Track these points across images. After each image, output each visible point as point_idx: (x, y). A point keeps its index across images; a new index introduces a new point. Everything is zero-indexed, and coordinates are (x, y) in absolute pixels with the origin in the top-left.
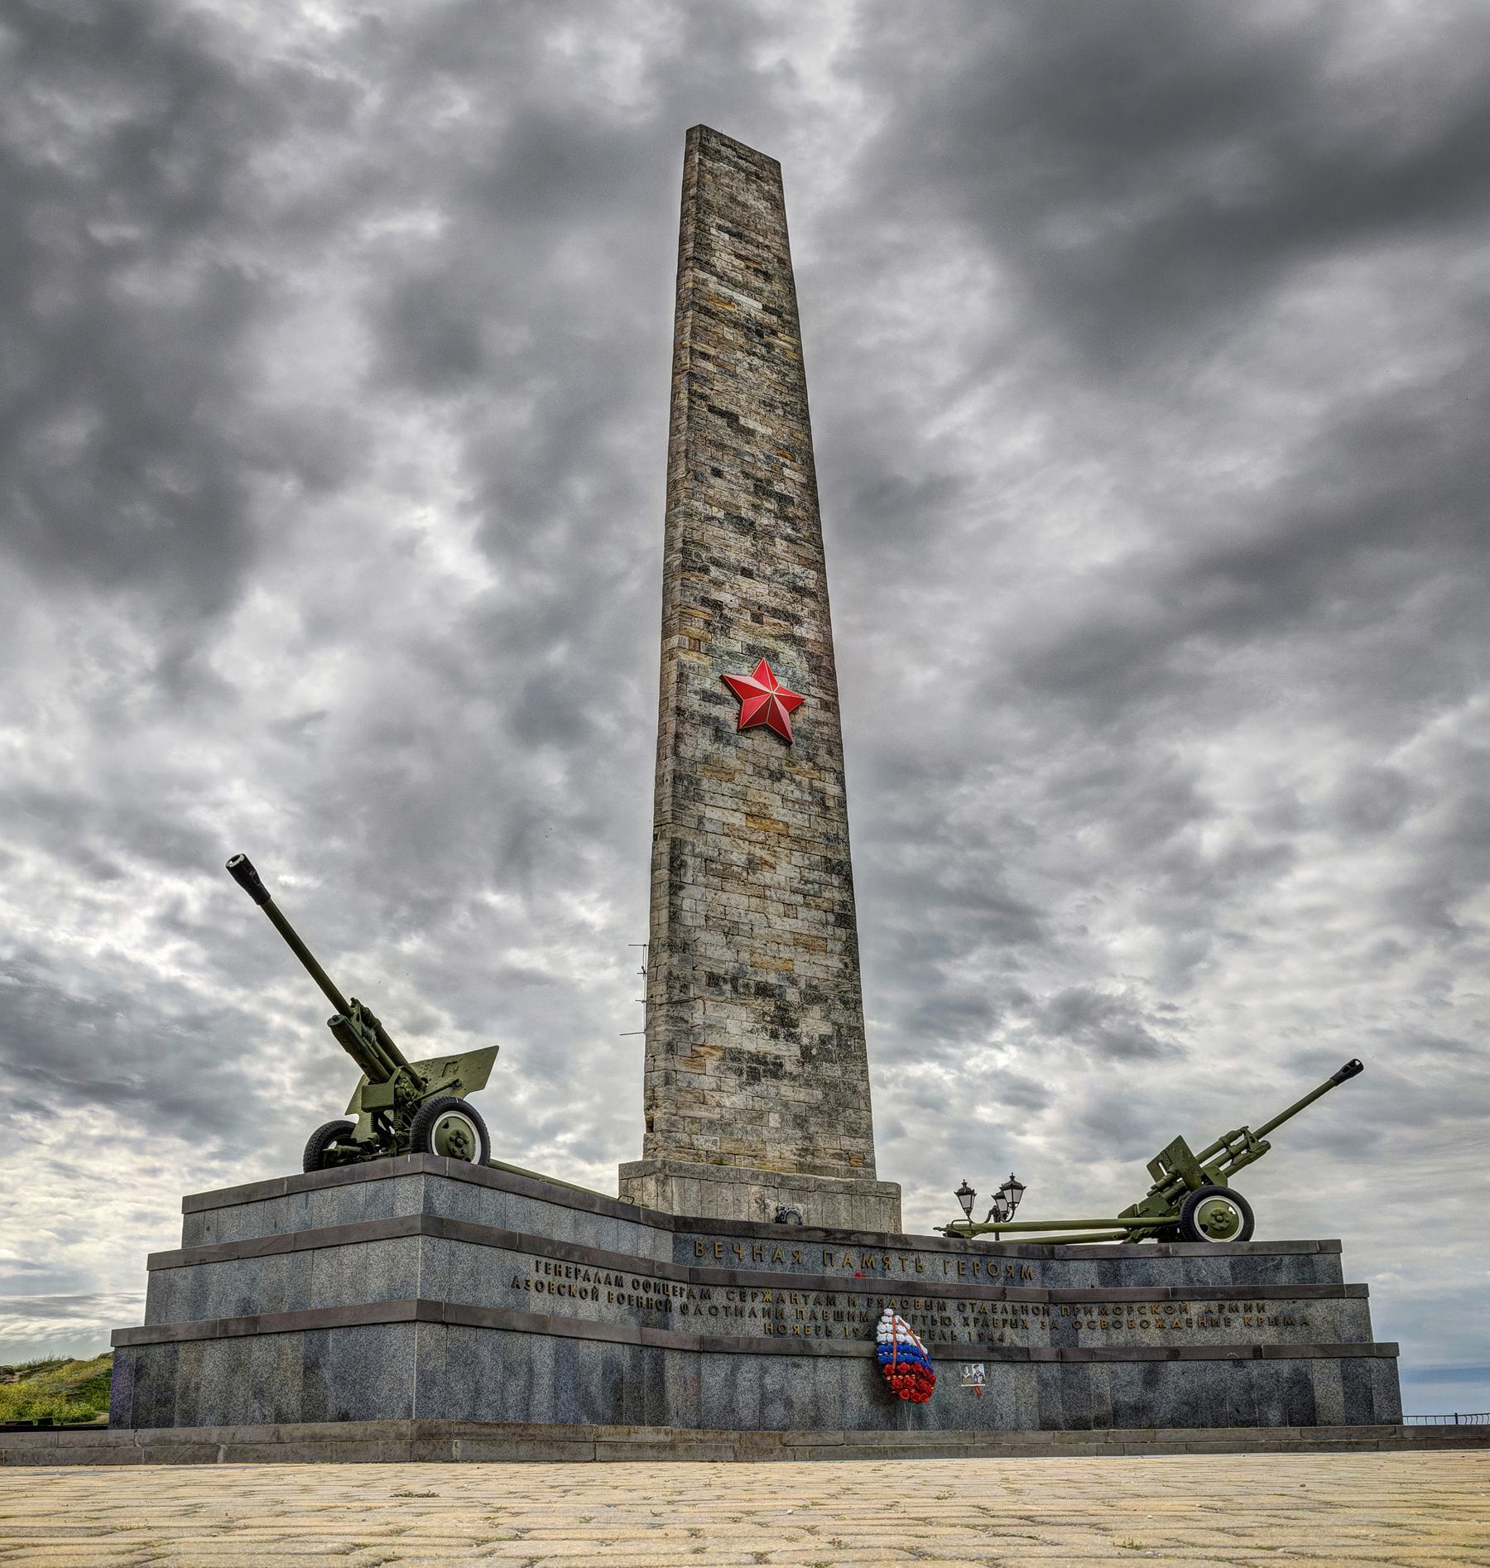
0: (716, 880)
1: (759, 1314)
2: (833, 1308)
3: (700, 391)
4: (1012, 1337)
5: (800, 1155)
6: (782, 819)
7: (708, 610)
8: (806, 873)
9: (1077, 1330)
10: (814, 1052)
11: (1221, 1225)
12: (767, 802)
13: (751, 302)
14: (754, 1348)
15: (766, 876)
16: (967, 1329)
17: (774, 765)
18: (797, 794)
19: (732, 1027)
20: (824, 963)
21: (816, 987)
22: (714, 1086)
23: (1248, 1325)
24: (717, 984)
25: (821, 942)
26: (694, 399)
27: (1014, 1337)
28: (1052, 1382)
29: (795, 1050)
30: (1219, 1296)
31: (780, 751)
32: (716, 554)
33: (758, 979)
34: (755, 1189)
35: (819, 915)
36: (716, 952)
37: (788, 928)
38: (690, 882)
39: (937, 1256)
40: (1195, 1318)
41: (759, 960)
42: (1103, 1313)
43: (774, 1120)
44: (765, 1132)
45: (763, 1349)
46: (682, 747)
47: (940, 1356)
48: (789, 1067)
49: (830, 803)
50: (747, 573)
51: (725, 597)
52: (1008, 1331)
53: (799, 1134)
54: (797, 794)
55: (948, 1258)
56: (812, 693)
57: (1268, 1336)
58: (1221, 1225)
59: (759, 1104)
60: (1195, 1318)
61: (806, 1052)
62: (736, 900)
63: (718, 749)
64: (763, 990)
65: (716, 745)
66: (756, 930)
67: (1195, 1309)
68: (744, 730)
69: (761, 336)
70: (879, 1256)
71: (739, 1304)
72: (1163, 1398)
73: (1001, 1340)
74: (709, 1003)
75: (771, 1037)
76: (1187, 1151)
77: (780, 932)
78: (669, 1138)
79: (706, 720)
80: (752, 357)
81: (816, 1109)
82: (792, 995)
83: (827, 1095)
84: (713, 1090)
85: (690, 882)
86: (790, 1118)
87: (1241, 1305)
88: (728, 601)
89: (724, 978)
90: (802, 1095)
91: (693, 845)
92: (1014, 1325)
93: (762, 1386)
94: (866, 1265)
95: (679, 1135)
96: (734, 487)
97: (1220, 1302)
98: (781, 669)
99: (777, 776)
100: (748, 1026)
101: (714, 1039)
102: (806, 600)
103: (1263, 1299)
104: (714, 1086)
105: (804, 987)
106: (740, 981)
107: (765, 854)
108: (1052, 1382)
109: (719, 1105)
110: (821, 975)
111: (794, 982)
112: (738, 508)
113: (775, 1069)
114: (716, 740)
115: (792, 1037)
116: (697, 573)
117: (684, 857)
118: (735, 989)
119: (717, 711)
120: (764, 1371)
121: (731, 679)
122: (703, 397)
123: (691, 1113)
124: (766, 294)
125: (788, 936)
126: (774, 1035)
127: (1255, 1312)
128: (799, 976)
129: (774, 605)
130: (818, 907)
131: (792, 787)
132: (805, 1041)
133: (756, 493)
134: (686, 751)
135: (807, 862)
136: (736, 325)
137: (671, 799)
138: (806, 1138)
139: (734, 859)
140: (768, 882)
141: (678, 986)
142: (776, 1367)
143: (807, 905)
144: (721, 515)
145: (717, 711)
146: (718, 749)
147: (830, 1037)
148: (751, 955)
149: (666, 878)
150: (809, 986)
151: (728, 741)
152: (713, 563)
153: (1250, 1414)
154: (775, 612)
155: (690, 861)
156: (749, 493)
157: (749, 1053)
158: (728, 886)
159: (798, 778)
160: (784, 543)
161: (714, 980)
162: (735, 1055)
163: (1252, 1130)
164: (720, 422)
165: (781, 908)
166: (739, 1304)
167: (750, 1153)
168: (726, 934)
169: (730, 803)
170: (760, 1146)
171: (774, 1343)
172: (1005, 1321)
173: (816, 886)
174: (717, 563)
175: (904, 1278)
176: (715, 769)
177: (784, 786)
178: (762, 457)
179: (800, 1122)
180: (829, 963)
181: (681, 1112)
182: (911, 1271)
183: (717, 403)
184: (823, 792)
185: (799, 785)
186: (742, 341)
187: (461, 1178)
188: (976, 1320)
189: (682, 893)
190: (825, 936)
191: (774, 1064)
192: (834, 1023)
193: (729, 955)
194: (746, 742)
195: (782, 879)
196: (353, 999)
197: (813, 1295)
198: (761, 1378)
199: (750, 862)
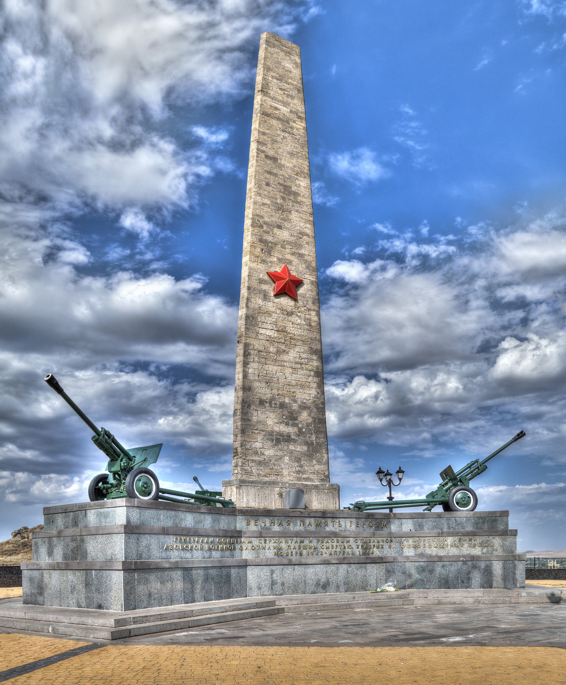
0: (263, 360)
1: (272, 548)
2: (302, 544)
3: (261, 149)
4: (377, 553)
5: (297, 473)
6: (293, 332)
7: (262, 244)
8: (302, 354)
10: (304, 430)
11: (464, 502)
12: (285, 325)
13: (285, 108)
14: (269, 563)
15: (285, 357)
16: (358, 550)
17: (289, 309)
18: (299, 321)
19: (270, 422)
20: (308, 392)
21: (305, 403)
22: (261, 446)
23: (470, 547)
24: (263, 404)
25: (308, 384)
26: (259, 152)
27: (377, 552)
28: (392, 570)
29: (296, 429)
31: (292, 303)
32: (266, 219)
33: (280, 401)
34: (277, 489)
35: (308, 373)
37: (293, 379)
38: (252, 361)
39: (347, 519)
40: (449, 544)
41: (281, 393)
43: (286, 459)
44: (282, 464)
45: (272, 563)
46: (250, 303)
47: (346, 562)
48: (293, 437)
49: (313, 324)
50: (279, 227)
51: (270, 238)
52: (375, 549)
53: (296, 464)
54: (299, 321)
55: (352, 520)
56: (306, 277)
58: (464, 502)
59: (280, 453)
61: (300, 430)
62: (272, 368)
63: (265, 303)
64: (282, 406)
65: (264, 302)
66: (280, 380)
67: (450, 540)
68: (277, 295)
69: (289, 123)
70: (323, 521)
71: (264, 545)
72: (434, 576)
73: (372, 553)
74: (259, 412)
75: (286, 424)
76: (452, 471)
77: (290, 381)
78: (243, 469)
79: (261, 291)
80: (284, 133)
81: (303, 454)
82: (295, 407)
84: (260, 448)
85: (252, 361)
86: (293, 458)
88: (271, 239)
89: (266, 402)
90: (299, 449)
91: (254, 345)
92: (378, 548)
93: (272, 578)
94: (318, 525)
95: (246, 468)
96: (275, 190)
98: (293, 268)
99: (290, 314)
100: (275, 420)
102: (305, 237)
104: (261, 446)
105: (300, 403)
106: (273, 402)
107: (283, 347)
108: (392, 570)
109: (263, 454)
110: (307, 398)
111: (295, 401)
112: (276, 199)
113: (288, 439)
114: (264, 300)
115: (294, 425)
116: (258, 228)
117: (250, 351)
118: (271, 406)
119: (264, 287)
120: (272, 572)
122: (263, 152)
123: (251, 458)
124: (291, 105)
125: (294, 382)
126: (287, 424)
127: (473, 541)
128: (298, 398)
129: (291, 240)
130: (307, 369)
131: (297, 318)
132: (300, 426)
133: (284, 193)
134: (251, 305)
135: (302, 350)
136: (278, 119)
137: (244, 326)
138: (300, 466)
139: (271, 350)
140: (286, 359)
141: (246, 405)
142: (278, 569)
143: (302, 368)
144: (269, 202)
145: (264, 287)
146: (265, 303)
147: (311, 423)
148: (278, 391)
151: (269, 300)
152: (265, 223)
153: (467, 584)
154: (289, 243)
155: (252, 352)
156: (280, 192)
157: (276, 432)
158: (268, 362)
159: (299, 314)
160: (296, 213)
161: (262, 402)
163: (480, 461)
165: (291, 370)
166: (264, 545)
167: (276, 473)
169: (270, 327)
170: (280, 470)
171: (277, 560)
172: (374, 546)
173: (306, 360)
174: (265, 223)
175: (333, 529)
176: (264, 312)
177: (294, 318)
178: (287, 176)
179: (298, 460)
180: (311, 392)
181: (247, 458)
182: (336, 526)
183: (269, 154)
184: (310, 319)
185: (300, 317)
186: (281, 126)
187: (142, 506)
188: (362, 546)
189: (248, 366)
190: (310, 381)
191: (287, 436)
192: (313, 418)
193: (268, 391)
195: (291, 358)
196: (102, 428)
197: (295, 539)
198: (272, 574)
199: (278, 351)
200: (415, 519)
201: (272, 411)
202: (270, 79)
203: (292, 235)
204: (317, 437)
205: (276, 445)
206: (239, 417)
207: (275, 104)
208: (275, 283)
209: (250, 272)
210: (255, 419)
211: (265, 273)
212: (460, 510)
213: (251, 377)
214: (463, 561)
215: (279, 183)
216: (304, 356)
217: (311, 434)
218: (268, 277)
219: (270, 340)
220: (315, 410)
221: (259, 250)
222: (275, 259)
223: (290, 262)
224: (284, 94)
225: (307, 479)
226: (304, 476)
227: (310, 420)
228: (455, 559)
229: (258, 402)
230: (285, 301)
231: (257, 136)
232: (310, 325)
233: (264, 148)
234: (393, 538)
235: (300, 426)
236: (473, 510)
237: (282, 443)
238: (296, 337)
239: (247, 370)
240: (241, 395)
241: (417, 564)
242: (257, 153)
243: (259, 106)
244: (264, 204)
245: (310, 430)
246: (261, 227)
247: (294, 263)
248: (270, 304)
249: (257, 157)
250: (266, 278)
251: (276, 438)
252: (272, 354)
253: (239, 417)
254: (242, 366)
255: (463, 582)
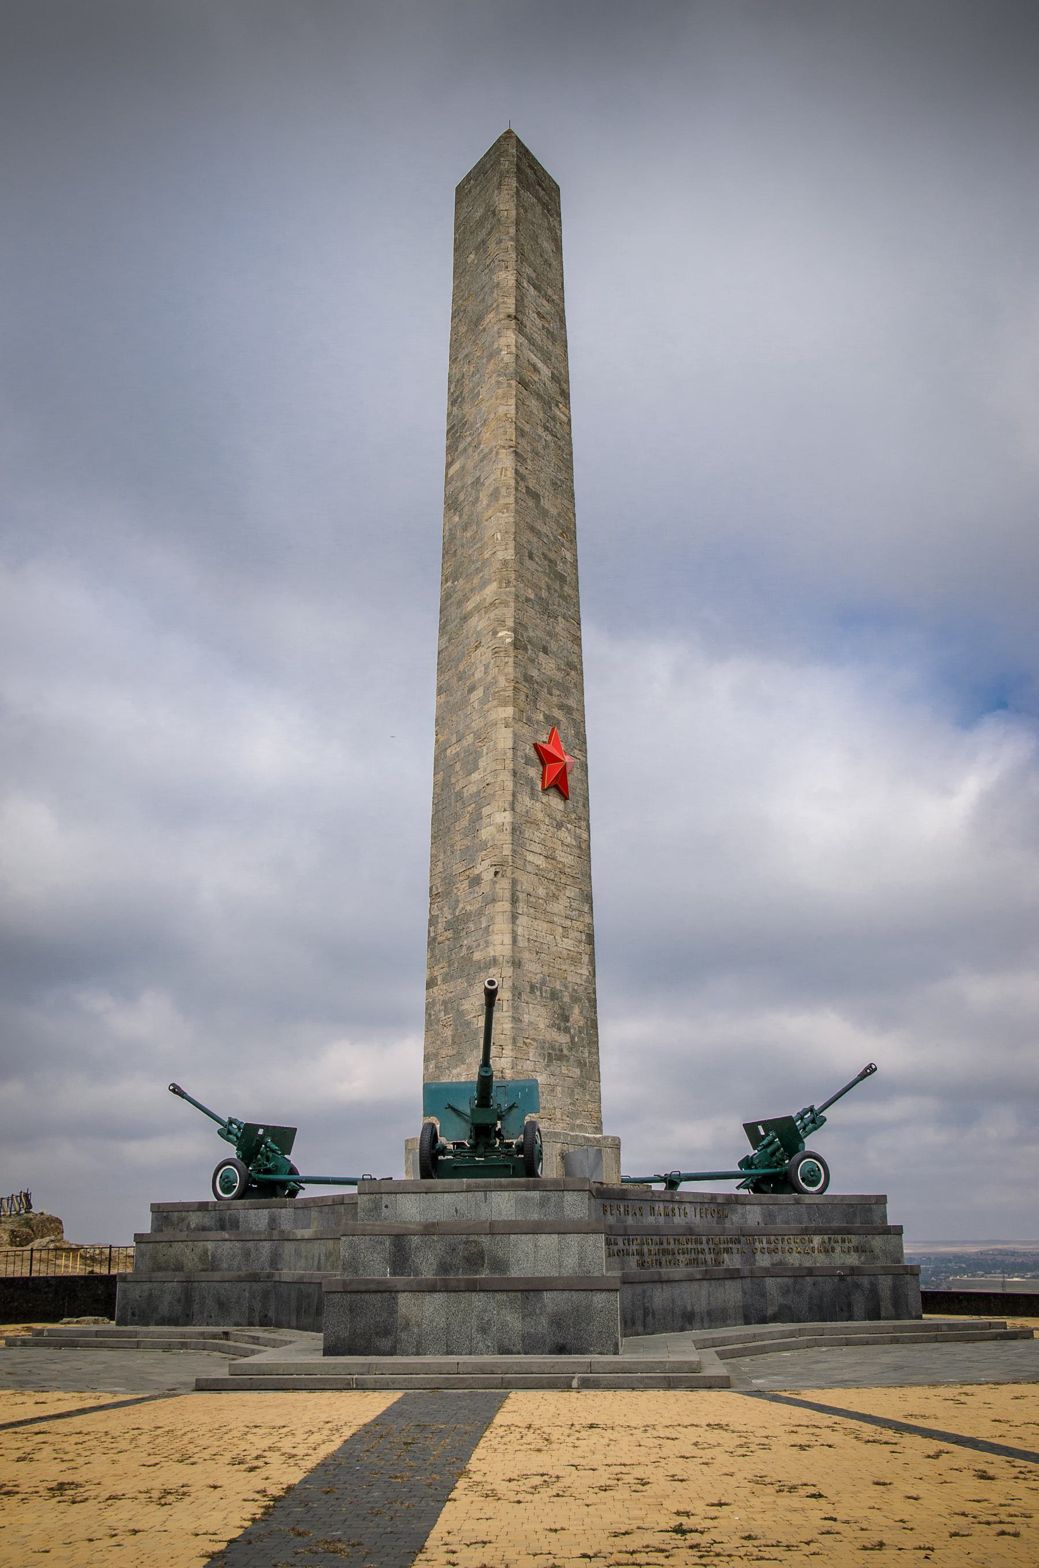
9: (755, 1253)
10: (576, 1040)
30: (829, 1232)
36: (533, 969)
40: (816, 1246)
41: (551, 971)
42: (769, 1242)
48: (565, 1052)
50: (545, 650)
51: (534, 673)
53: (569, 1101)
57: (853, 1260)
59: (552, 1081)
60: (816, 1246)
61: (572, 1038)
64: (554, 995)
67: (817, 1240)
83: (582, 1071)
84: (532, 1071)
87: (839, 1237)
97: (829, 1236)
99: (559, 826)
101: (532, 1033)
103: (851, 1234)
111: (566, 987)
115: (567, 1030)
121: (542, 748)
134: (519, 808)
144: (532, 597)
149: (509, 909)
150: (574, 990)
151: (537, 797)
154: (558, 685)
162: (542, 1044)
164: (531, 503)
168: (537, 953)
169: (537, 848)
177: (563, 834)
189: (518, 922)
194: (545, 799)
200: (765, 1206)
201: (543, 1004)
202: (525, 285)
203: (559, 669)
204: (590, 1053)
205: (548, 1066)
206: (507, 1014)
207: (533, 357)
208: (543, 764)
209: (515, 742)
210: (526, 1018)
211: (531, 742)
212: (806, 1192)
213: (522, 943)
214: (840, 1275)
215: (543, 554)
216: (575, 905)
217: (584, 1047)
218: (536, 754)
219: (539, 873)
220: (587, 1005)
221: (523, 697)
222: (541, 717)
223: (559, 723)
224: (543, 326)
225: (581, 1127)
226: (578, 1122)
227: (581, 1023)
228: (828, 1273)
229: (528, 989)
230: (555, 801)
231: (513, 438)
232: (580, 847)
233: (522, 470)
234: (741, 1237)
235: (572, 1031)
236: (821, 1193)
237: (554, 1061)
238: (567, 870)
239: (515, 929)
240: (510, 974)
241: (779, 1280)
242: (517, 482)
243: (513, 360)
244: (528, 600)
245: (583, 1039)
246: (525, 649)
247: (563, 727)
248: (538, 805)
249: (516, 489)
250: (533, 754)
251: (548, 1053)
252: (540, 900)
253: (507, 1014)
254: (510, 920)
255: (842, 1310)
